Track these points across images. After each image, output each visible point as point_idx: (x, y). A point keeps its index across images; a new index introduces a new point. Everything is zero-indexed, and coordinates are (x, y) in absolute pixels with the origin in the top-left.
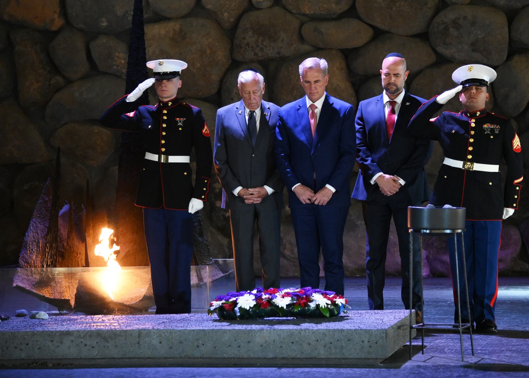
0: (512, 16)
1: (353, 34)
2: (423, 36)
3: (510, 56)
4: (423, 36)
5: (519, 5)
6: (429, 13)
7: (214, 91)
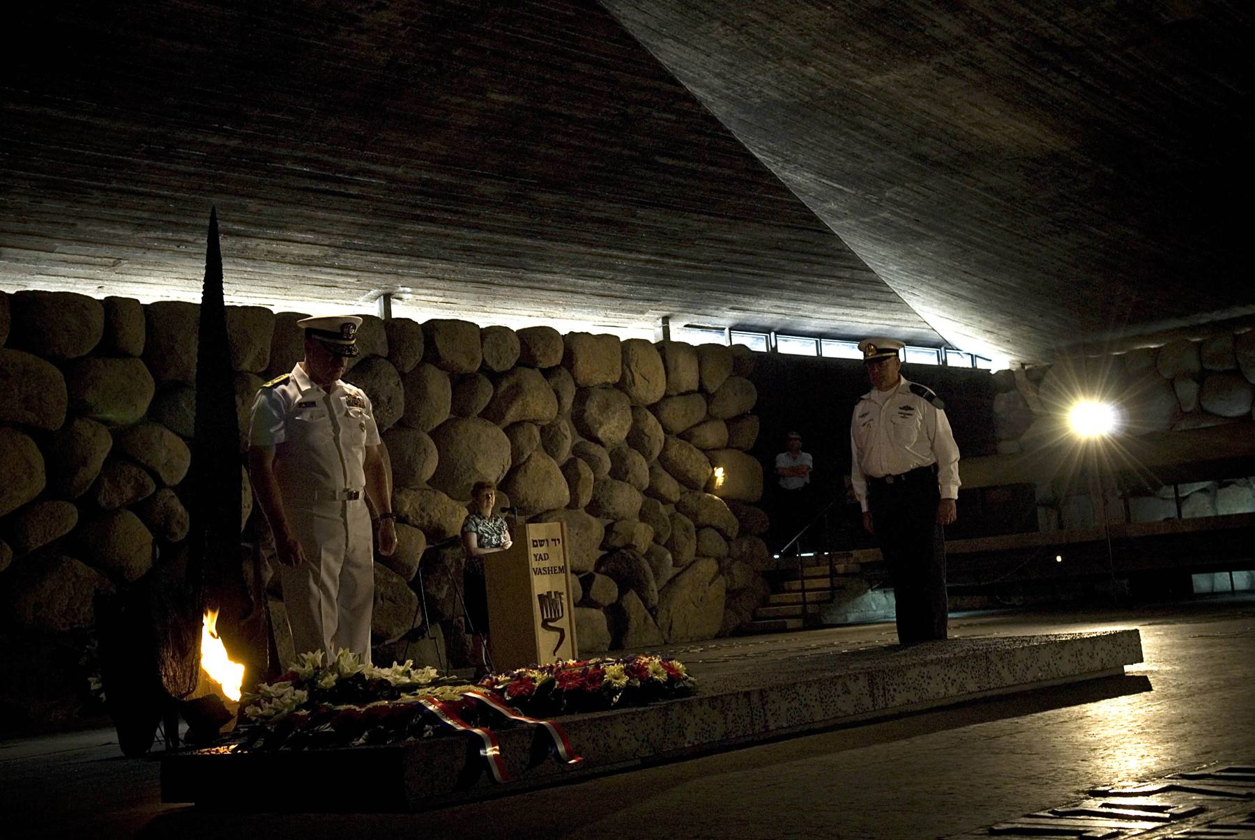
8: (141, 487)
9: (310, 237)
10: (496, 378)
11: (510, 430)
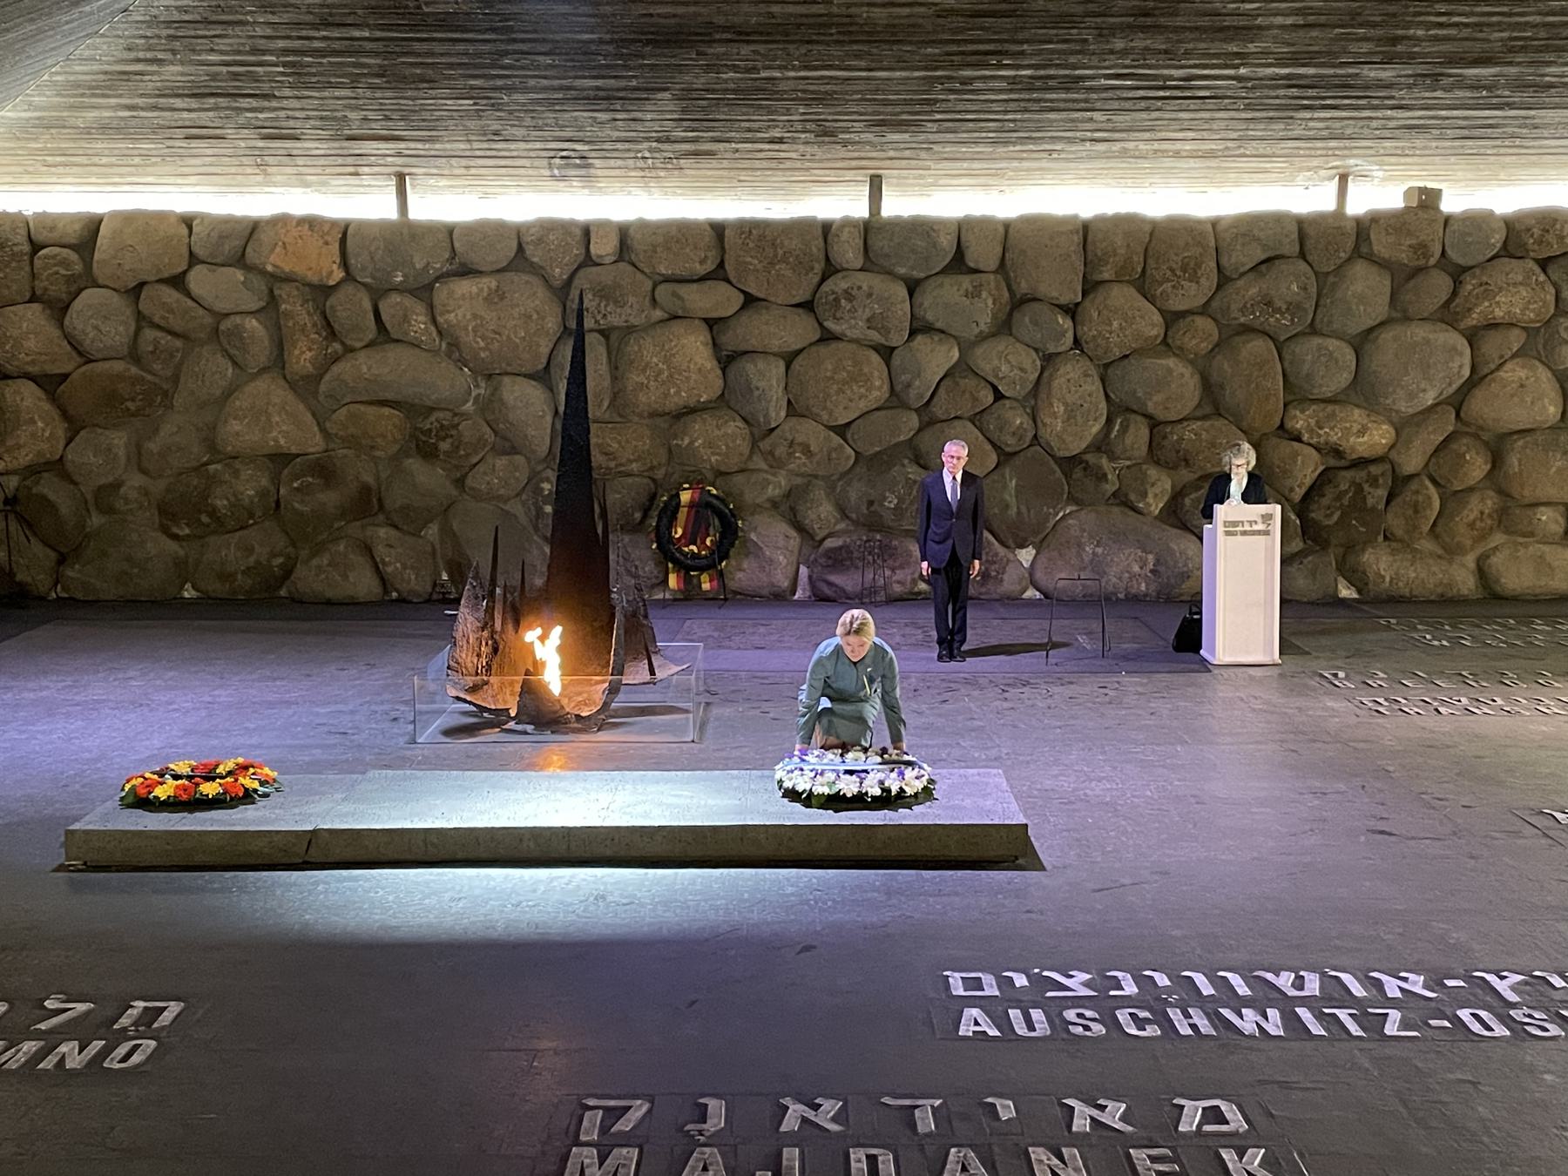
0: (913, 287)
1: (719, 300)
2: (808, 306)
3: (913, 333)
4: (808, 306)
5: (922, 275)
6: (816, 279)
7: (541, 367)
8: (975, 399)
9: (1191, 135)
10: (1458, 274)
11: (1472, 337)
